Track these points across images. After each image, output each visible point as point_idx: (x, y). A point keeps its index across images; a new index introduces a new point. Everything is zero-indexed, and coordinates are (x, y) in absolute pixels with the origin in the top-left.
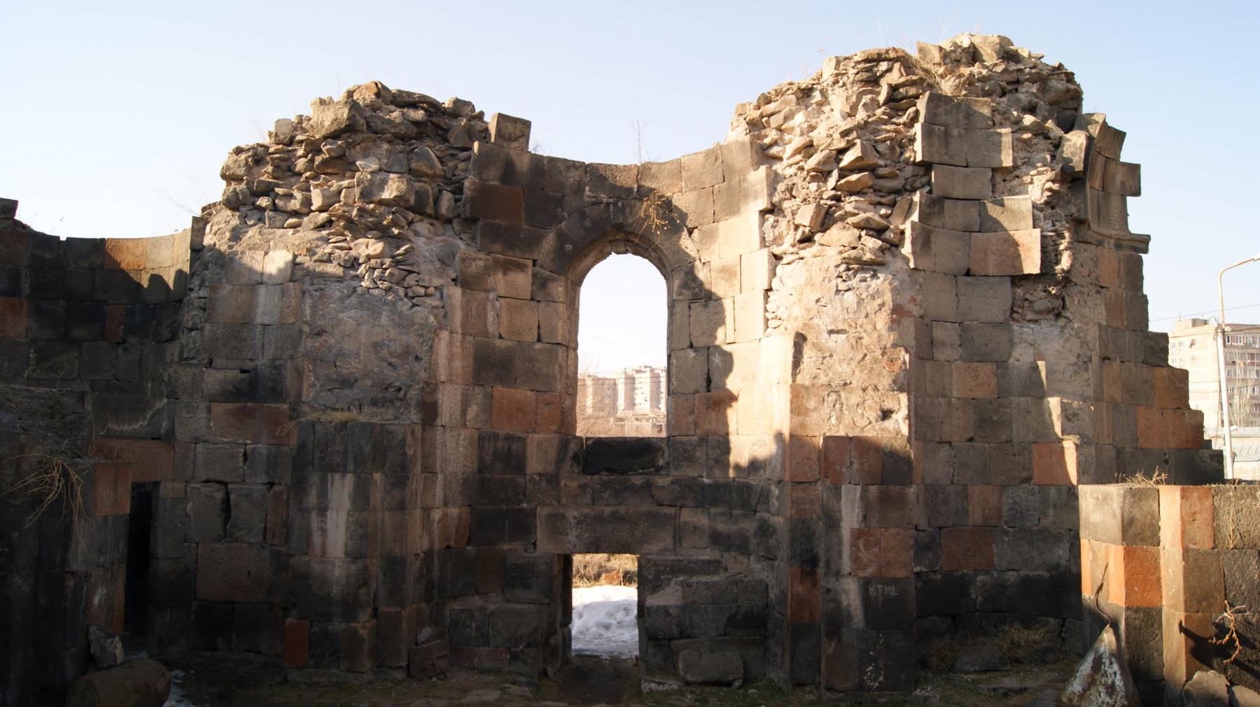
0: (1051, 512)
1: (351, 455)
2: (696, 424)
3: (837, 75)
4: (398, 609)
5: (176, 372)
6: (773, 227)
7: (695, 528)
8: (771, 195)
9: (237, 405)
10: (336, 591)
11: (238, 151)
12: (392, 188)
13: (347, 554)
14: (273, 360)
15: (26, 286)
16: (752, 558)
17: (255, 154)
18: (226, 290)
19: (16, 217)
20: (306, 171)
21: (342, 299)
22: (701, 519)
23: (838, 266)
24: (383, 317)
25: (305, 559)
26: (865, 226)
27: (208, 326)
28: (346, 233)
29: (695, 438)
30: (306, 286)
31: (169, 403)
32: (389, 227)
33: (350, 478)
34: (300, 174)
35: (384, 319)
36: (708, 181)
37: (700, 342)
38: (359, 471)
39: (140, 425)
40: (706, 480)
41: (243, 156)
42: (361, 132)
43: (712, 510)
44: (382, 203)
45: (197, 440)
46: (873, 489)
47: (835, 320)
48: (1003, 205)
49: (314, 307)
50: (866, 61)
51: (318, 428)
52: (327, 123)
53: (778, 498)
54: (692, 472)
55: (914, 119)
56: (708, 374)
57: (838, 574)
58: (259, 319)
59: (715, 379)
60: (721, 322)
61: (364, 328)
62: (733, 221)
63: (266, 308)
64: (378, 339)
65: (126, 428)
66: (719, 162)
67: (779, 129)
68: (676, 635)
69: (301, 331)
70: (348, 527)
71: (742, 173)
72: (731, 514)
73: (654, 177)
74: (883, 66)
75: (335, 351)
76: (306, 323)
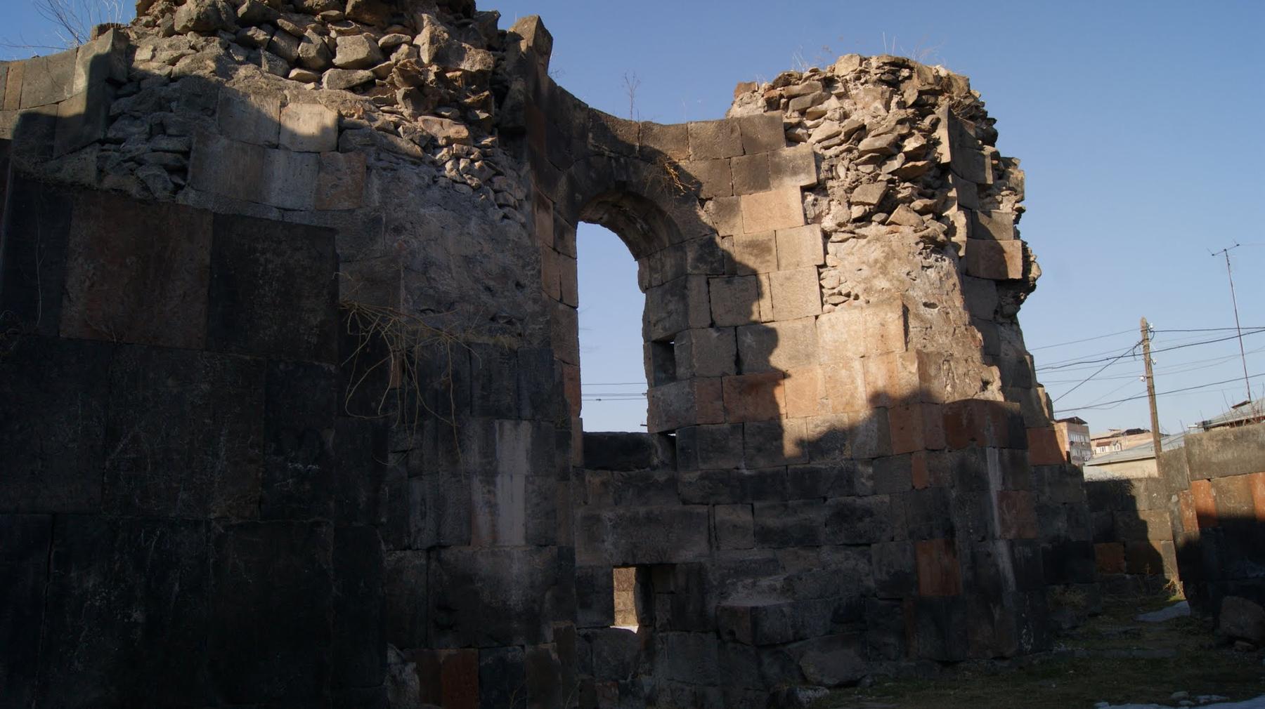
0: (1047, 489)
2: (726, 410)
3: (861, 71)
4: (568, 623)
6: (814, 205)
7: (735, 526)
8: (818, 172)
10: (515, 598)
13: (527, 539)
16: (825, 548)
18: (220, 144)
22: (742, 516)
23: (917, 244)
24: (473, 223)
25: (468, 550)
26: (922, 212)
29: (726, 426)
33: (526, 426)
35: (473, 226)
36: (722, 153)
37: (725, 320)
38: (538, 417)
40: (746, 472)
43: (757, 505)
46: (1005, 451)
47: (926, 294)
48: (990, 216)
49: (384, 191)
50: (891, 64)
53: (871, 477)
54: (726, 464)
55: (935, 125)
56: (738, 355)
57: (993, 538)
59: (748, 359)
60: (759, 295)
62: (761, 195)
66: (736, 134)
67: (803, 113)
68: (791, 638)
70: (527, 501)
71: (774, 150)
72: (786, 506)
73: (656, 138)
74: (905, 73)
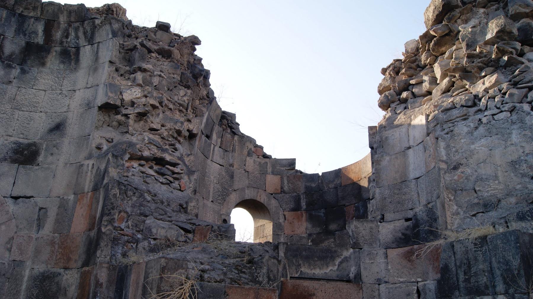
1: (498, 272)
5: (356, 227)
9: (406, 249)
11: (384, 71)
12: (492, 29)
14: (426, 205)
15: (303, 204)
17: (395, 67)
19: (298, 167)
20: (427, 58)
21: (471, 133)
27: (378, 191)
28: (465, 82)
30: (438, 133)
31: (354, 252)
32: (498, 59)
34: (425, 66)
35: (515, 137)
38: (511, 291)
39: (331, 270)
41: (387, 73)
42: (457, 7)
44: (487, 43)
45: (379, 282)
49: (448, 147)
51: (457, 247)
52: (431, 17)
58: (412, 175)
61: (497, 153)
63: (416, 164)
64: (514, 157)
65: (318, 272)
69: (440, 169)
75: (472, 179)
76: (443, 161)
